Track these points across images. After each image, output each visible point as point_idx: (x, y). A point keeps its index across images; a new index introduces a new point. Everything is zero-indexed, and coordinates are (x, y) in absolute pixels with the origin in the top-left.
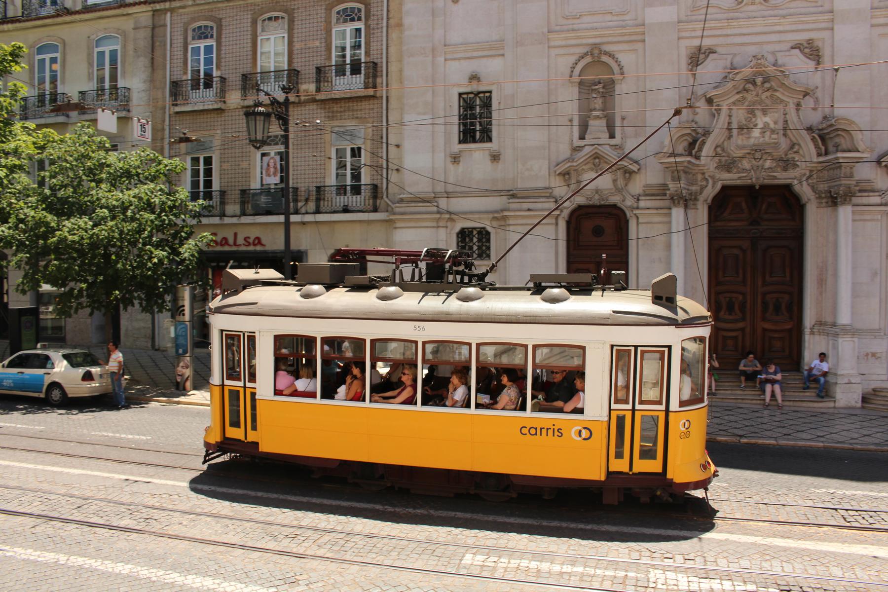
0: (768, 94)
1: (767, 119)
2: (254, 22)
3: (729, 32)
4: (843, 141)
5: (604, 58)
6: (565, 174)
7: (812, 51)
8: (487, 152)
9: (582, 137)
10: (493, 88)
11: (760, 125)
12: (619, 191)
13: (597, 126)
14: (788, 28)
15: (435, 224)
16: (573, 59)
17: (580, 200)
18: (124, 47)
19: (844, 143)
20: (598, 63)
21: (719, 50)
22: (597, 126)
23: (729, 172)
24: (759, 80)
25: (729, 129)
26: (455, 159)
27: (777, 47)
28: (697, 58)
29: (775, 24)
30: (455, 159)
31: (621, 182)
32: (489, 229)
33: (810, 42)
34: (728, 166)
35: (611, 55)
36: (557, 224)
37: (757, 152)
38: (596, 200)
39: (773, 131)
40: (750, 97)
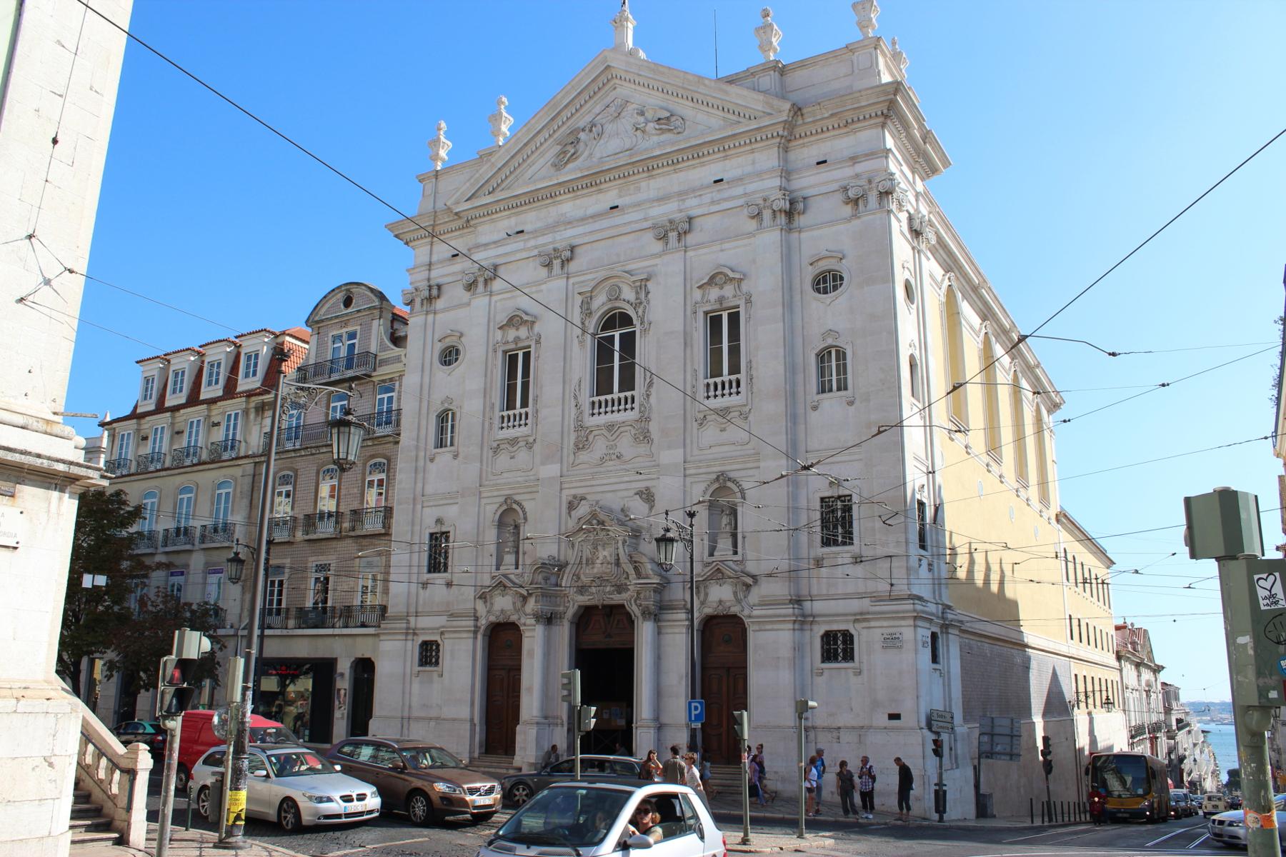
1: (606, 553)
2: (318, 473)
3: (593, 483)
5: (515, 506)
6: (483, 597)
7: (647, 496)
10: (451, 529)
12: (517, 611)
13: (509, 559)
17: (493, 619)
18: (235, 490)
22: (509, 559)
25: (581, 563)
27: (625, 494)
31: (519, 604)
33: (647, 489)
34: (582, 590)
35: (519, 504)
36: (475, 638)
37: (600, 580)
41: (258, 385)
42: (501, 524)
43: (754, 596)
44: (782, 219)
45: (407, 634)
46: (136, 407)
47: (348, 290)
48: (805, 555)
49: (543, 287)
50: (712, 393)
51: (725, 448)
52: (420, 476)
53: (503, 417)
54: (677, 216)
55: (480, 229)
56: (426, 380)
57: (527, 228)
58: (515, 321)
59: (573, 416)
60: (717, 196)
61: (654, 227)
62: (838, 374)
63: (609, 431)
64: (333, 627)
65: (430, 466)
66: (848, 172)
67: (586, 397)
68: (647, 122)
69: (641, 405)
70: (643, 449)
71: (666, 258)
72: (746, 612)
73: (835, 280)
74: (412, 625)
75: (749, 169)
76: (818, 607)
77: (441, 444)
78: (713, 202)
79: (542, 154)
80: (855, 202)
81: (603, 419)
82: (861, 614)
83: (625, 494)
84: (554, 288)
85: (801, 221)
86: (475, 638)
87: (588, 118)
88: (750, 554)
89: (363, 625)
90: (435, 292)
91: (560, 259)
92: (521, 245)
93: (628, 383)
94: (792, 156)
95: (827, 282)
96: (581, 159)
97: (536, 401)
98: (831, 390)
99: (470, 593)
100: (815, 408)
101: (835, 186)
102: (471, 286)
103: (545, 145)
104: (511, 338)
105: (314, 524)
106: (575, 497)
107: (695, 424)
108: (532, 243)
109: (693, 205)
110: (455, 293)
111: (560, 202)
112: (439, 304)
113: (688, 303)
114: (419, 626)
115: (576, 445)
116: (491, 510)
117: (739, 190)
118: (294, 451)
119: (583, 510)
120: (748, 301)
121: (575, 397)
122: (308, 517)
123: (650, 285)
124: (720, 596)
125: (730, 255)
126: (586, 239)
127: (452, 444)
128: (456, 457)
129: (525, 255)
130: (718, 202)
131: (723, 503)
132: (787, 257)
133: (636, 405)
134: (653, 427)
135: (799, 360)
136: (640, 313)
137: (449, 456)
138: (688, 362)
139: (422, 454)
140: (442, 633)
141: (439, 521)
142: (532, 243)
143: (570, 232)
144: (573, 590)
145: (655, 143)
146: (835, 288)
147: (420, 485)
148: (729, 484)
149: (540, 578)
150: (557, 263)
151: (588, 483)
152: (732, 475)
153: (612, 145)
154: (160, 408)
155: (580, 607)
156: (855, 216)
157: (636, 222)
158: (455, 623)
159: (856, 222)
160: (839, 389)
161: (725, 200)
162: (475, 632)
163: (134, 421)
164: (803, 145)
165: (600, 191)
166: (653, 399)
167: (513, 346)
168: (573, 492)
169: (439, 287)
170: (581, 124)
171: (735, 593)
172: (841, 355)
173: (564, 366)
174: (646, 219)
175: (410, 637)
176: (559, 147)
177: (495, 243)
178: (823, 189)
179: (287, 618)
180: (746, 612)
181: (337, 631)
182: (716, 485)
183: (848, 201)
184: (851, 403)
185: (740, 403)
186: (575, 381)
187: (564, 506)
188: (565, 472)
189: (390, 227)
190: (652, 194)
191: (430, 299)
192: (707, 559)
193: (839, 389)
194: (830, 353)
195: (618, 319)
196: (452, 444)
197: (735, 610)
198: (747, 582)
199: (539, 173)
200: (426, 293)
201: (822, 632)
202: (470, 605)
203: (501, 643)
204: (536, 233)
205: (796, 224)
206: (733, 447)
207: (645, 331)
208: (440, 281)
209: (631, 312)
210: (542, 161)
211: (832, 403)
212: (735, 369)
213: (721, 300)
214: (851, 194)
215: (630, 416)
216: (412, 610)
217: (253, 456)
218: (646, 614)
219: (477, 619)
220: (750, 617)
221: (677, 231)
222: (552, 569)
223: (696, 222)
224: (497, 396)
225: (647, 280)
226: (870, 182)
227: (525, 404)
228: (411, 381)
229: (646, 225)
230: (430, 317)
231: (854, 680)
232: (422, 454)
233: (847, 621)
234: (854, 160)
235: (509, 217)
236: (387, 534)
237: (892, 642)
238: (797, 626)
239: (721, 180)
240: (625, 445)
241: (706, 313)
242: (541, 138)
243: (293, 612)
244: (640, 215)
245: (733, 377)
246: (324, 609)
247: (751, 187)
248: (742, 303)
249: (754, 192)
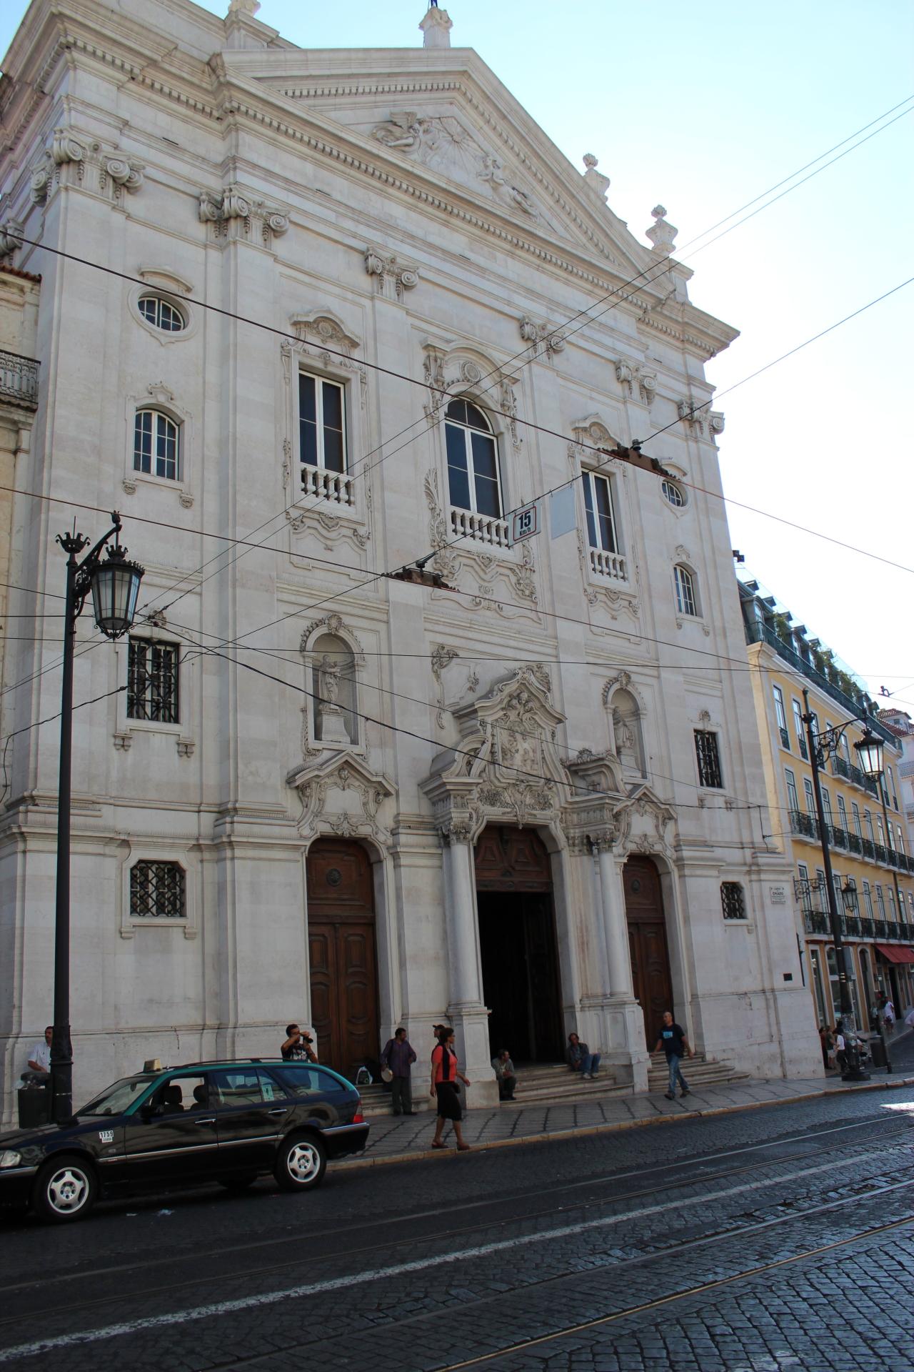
0: (528, 715)
1: (526, 745)
3: (470, 635)
4: (603, 780)
5: (342, 633)
6: (302, 790)
8: (173, 739)
9: (318, 736)
11: (521, 752)
13: (332, 723)
14: (521, 645)
16: (305, 624)
17: (324, 828)
19: (604, 782)
20: (332, 638)
23: (493, 805)
24: (525, 696)
26: (123, 742)
28: (442, 657)
30: (123, 742)
32: (184, 864)
38: (345, 830)
40: (513, 715)
111: (389, 197)
143: (407, 250)
150: (389, 281)
151: (461, 633)
157: (497, 298)
165: (446, 224)
168: (440, 639)
171: (657, 827)
174: (509, 303)
177: (286, 180)
182: (616, 686)
190: (501, 271)
191: (123, 185)
203: (343, 876)
229: (506, 309)
230: (118, 218)
231: (750, 939)
235: (303, 158)
242: (365, 85)
244: (502, 293)
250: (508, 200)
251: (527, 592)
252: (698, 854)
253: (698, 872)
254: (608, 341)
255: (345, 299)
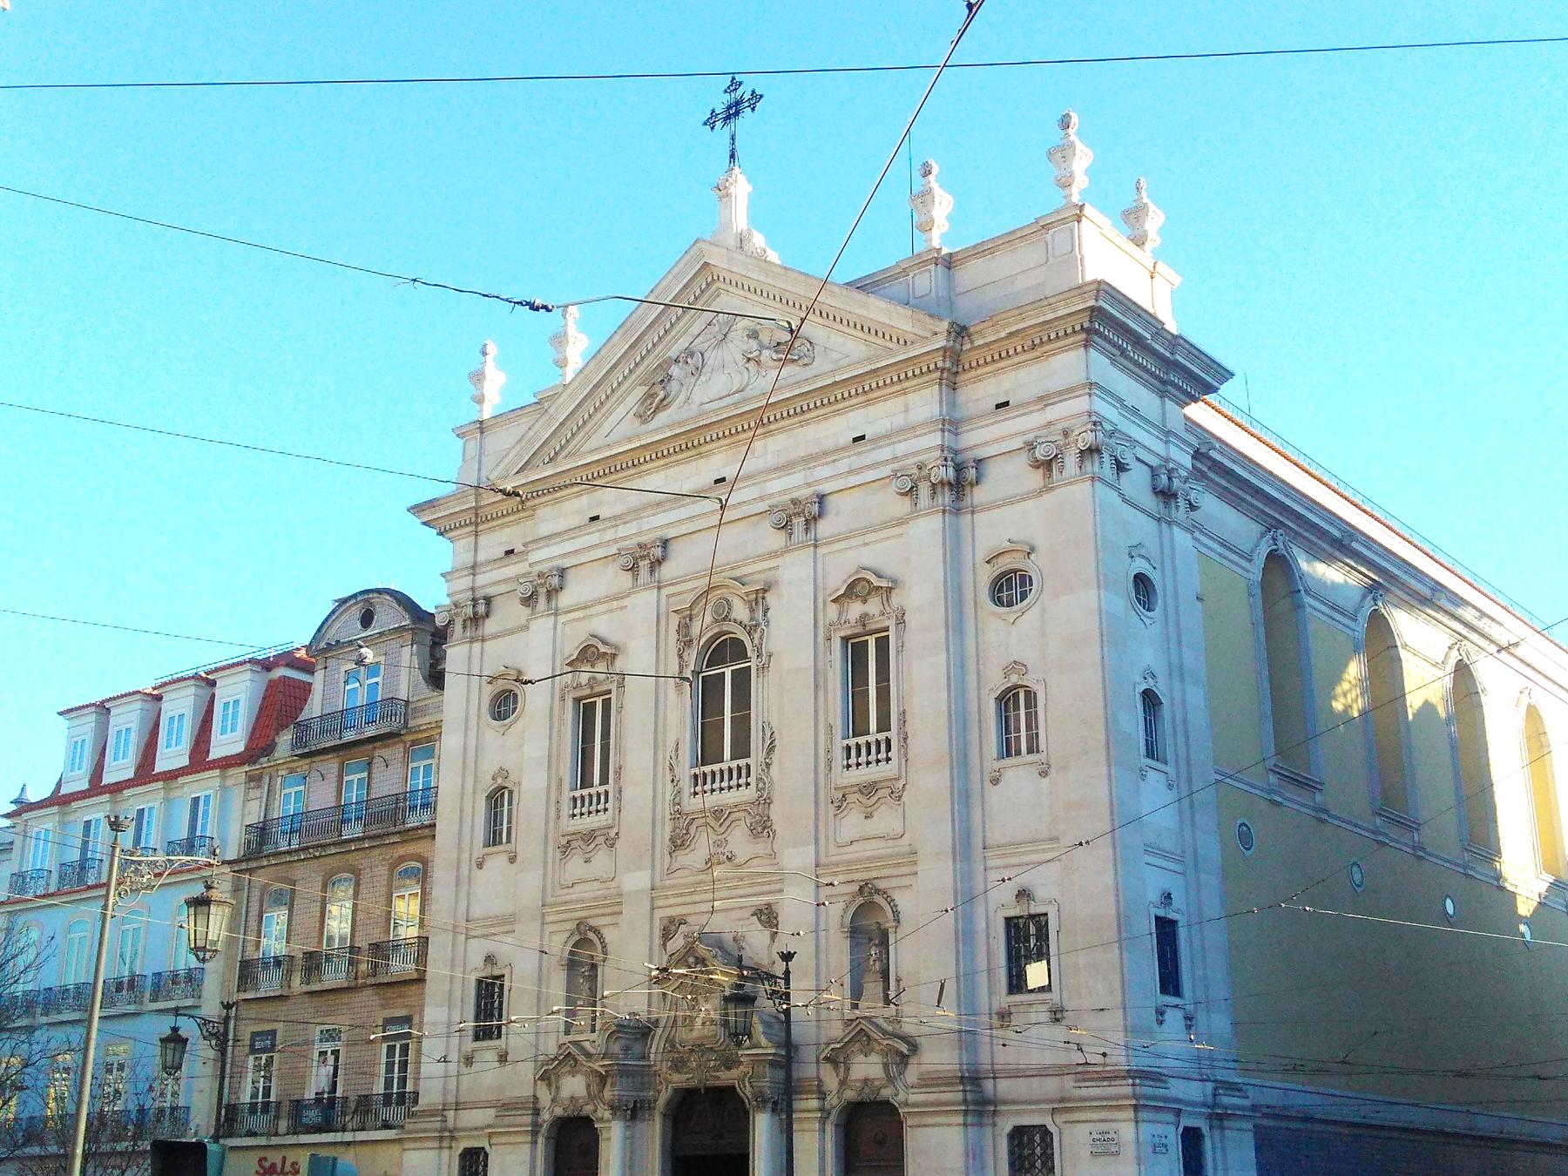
1: (708, 1006)
3: (697, 898)
5: (591, 935)
6: (545, 1077)
7: (768, 916)
10: (506, 972)
12: (591, 1097)
15: (436, 1144)
21: (689, 919)
26: (469, 1060)
29: (736, 887)
31: (594, 1088)
33: (769, 906)
34: (678, 1065)
35: (596, 931)
36: (534, 1143)
39: (712, 1021)
41: (240, 748)
42: (572, 965)
43: (911, 1074)
44: (946, 497)
45: (441, 1138)
46: (59, 785)
47: (367, 600)
48: (984, 1008)
49: (626, 602)
50: (853, 761)
51: (873, 844)
52: (464, 889)
53: (575, 799)
54: (804, 493)
55: (540, 513)
56: (472, 742)
57: (603, 512)
58: (591, 653)
59: (668, 797)
60: (857, 462)
61: (769, 511)
62: (1029, 727)
63: (717, 819)
64: (344, 1130)
65: (480, 875)
66: (1036, 419)
67: (685, 771)
68: (762, 347)
69: (759, 780)
70: (761, 847)
71: (788, 558)
72: (902, 1097)
73: (1023, 584)
74: (450, 1123)
75: (899, 421)
76: (1005, 1087)
77: (494, 838)
78: (851, 472)
79: (622, 400)
80: (1046, 465)
81: (712, 800)
82: (1062, 1100)
83: (739, 914)
84: (644, 603)
85: (979, 495)
86: (534, 1143)
87: (683, 343)
88: (907, 1009)
89: (386, 1126)
90: (481, 609)
91: (647, 559)
92: (594, 539)
93: (742, 748)
94: (963, 394)
95: (1010, 587)
96: (673, 407)
97: (618, 773)
98: (1018, 753)
99: (527, 1071)
100: (995, 781)
101: (1018, 443)
102: (529, 600)
103: (623, 388)
104: (584, 678)
105: (318, 967)
106: (671, 920)
107: (832, 808)
108: (610, 535)
109: (824, 477)
110: (508, 612)
112: (490, 626)
113: (821, 623)
114: (460, 1124)
115: (672, 840)
116: (559, 945)
117: (885, 453)
118: (289, 852)
119: (678, 942)
120: (901, 621)
121: (672, 769)
122: (309, 956)
123: (770, 598)
124: (866, 1067)
125: (877, 554)
126: (683, 529)
127: (509, 841)
128: (512, 860)
129: (600, 553)
130: (859, 470)
131: (869, 930)
132: (954, 549)
133: (752, 780)
134: (776, 812)
135: (973, 707)
136: (756, 641)
137: (504, 858)
138: (821, 713)
139: (466, 855)
140: (490, 1135)
141: (490, 959)
142: (610, 535)
143: (662, 518)
144: (665, 1066)
145: (764, 382)
146: (1024, 596)
147: (463, 905)
148: (878, 899)
149: (616, 1048)
152: (881, 885)
153: (722, 382)
154: (97, 787)
155: (676, 1090)
156: (1047, 489)
158: (507, 1120)
159: (1048, 498)
160: (1030, 751)
161: (868, 467)
162: (535, 1133)
163: (55, 809)
164: (979, 379)
166: (774, 770)
167: (587, 692)
169: (488, 600)
170: (673, 353)
171: (886, 1066)
172: (1031, 697)
173: (654, 722)
174: (762, 498)
175: (446, 1144)
176: (644, 389)
178: (1005, 447)
179: (277, 1117)
180: (902, 1097)
181: (348, 1137)
183: (1037, 464)
184: (1044, 774)
185: (890, 775)
186: (671, 744)
187: (657, 934)
188: (658, 883)
189: (417, 509)
192: (848, 1014)
193: (1030, 751)
194: (1016, 696)
195: (726, 649)
196: (509, 841)
197: (886, 1093)
198: (903, 1051)
199: (618, 427)
200: (469, 611)
201: (1008, 1128)
202: (527, 1091)
204: (617, 519)
205: (967, 501)
206: (881, 843)
207: (763, 669)
208: (490, 591)
209: (744, 637)
210: (621, 410)
211: (1019, 776)
212: (884, 725)
213: (864, 619)
214: (1039, 453)
215: (748, 794)
216: (451, 1099)
217: (230, 863)
218: (762, 1101)
219: (537, 1112)
220: (907, 1104)
221: (803, 517)
222: (641, 1032)
223: (832, 502)
224: (567, 767)
225: (765, 591)
226: (1066, 434)
227: (604, 780)
228: (450, 743)
229: (763, 506)
230: (477, 646)
232: (466, 855)
233: (1041, 1111)
234: (1044, 400)
236: (420, 980)
237: (1105, 1147)
238: (970, 1119)
239: (863, 437)
240: (739, 841)
241: (845, 639)
243: (286, 1107)
245: (882, 736)
246: (332, 1101)
247: (901, 448)
248: (891, 624)
249: (906, 456)
250: (772, 363)
251: (762, 827)
252: (932, 1097)
253: (930, 1120)
254: (885, 453)
255: (611, 611)
